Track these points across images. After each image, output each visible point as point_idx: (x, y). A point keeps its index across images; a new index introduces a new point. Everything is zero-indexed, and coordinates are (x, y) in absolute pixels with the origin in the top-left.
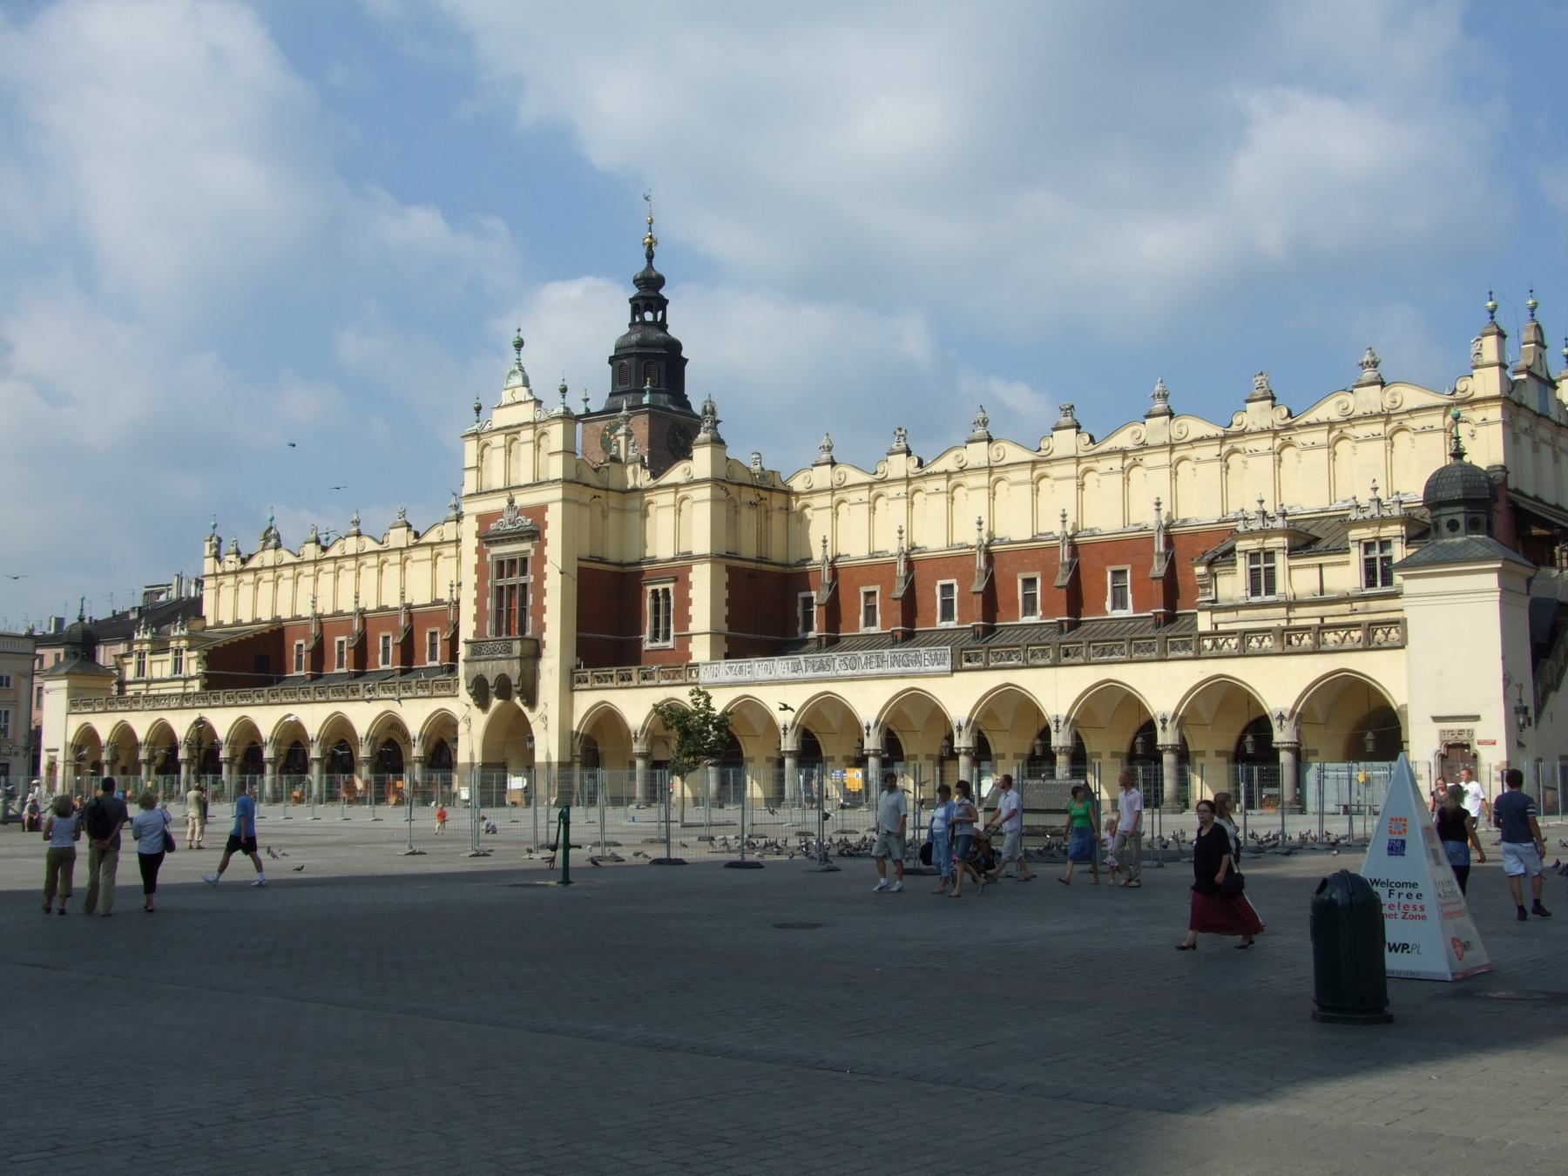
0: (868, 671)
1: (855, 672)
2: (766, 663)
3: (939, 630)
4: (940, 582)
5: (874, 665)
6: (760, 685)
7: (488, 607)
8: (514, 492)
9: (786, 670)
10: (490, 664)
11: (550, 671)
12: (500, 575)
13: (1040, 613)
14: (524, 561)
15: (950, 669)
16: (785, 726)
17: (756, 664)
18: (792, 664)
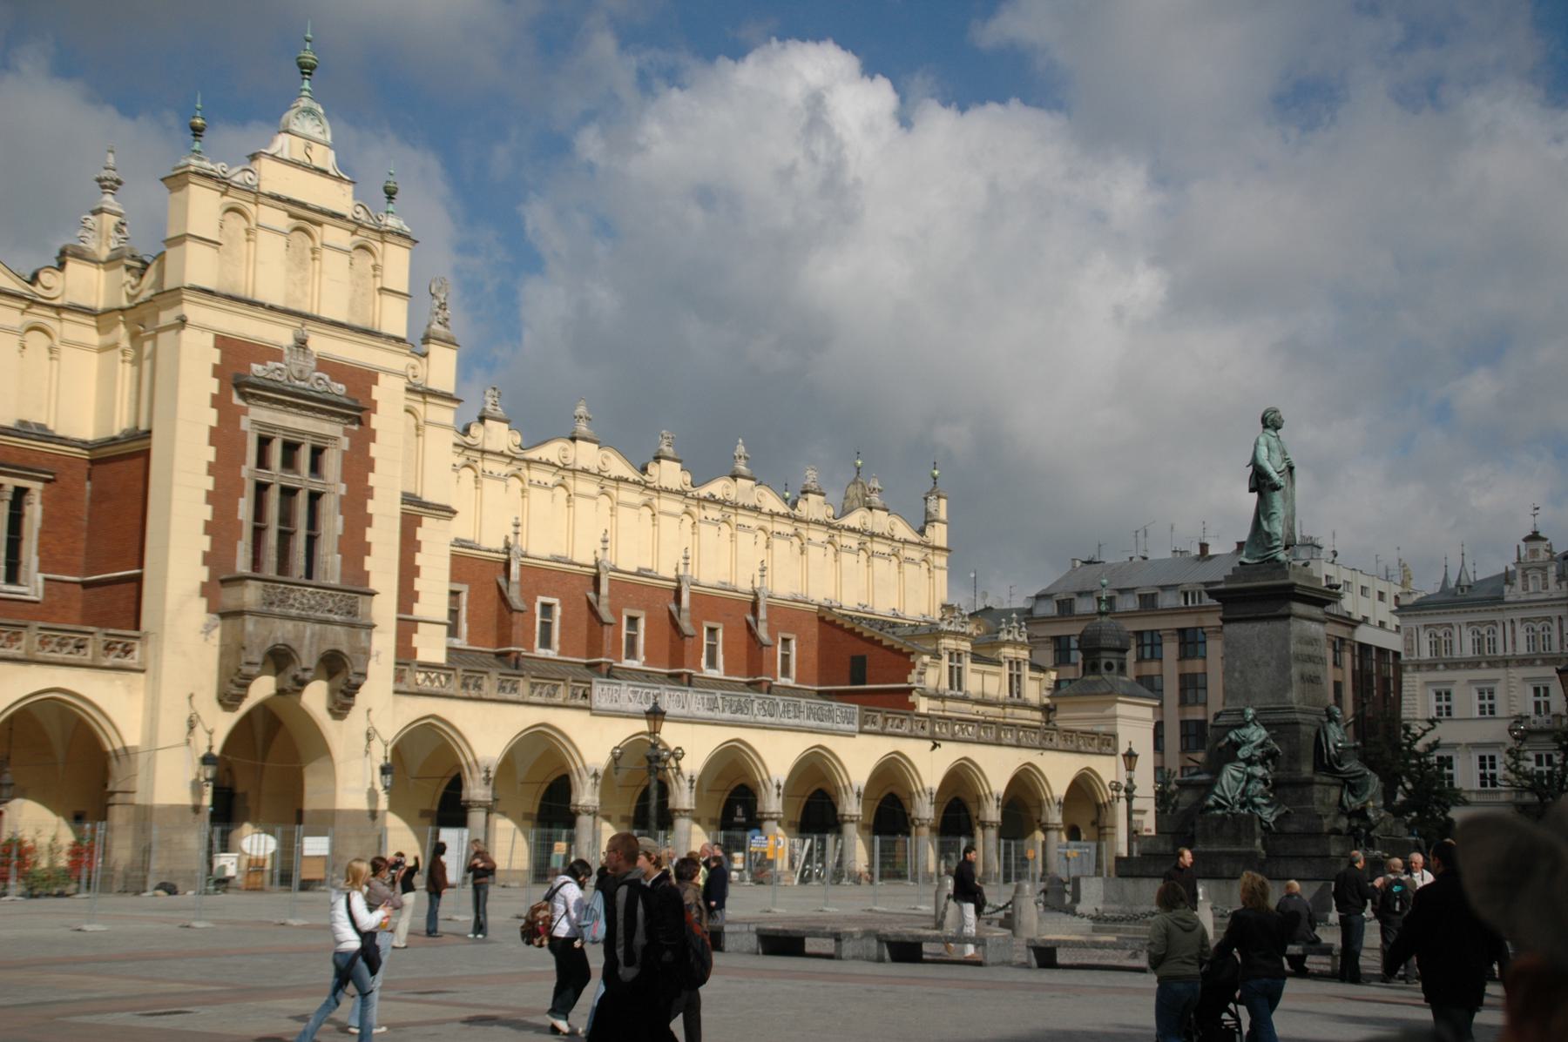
0: (786, 721)
1: (773, 720)
2: (678, 693)
3: (535, 658)
4: (541, 599)
5: (792, 714)
6: (716, 724)
7: (240, 517)
8: (311, 326)
9: (701, 706)
10: (309, 629)
11: (377, 655)
12: (262, 462)
13: (643, 659)
14: (317, 452)
15: (857, 730)
16: (692, 777)
17: (667, 693)
18: (708, 699)
